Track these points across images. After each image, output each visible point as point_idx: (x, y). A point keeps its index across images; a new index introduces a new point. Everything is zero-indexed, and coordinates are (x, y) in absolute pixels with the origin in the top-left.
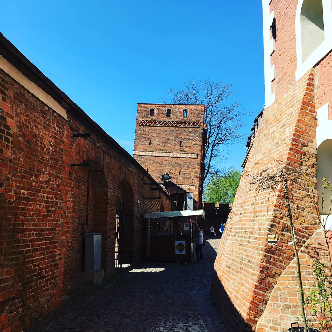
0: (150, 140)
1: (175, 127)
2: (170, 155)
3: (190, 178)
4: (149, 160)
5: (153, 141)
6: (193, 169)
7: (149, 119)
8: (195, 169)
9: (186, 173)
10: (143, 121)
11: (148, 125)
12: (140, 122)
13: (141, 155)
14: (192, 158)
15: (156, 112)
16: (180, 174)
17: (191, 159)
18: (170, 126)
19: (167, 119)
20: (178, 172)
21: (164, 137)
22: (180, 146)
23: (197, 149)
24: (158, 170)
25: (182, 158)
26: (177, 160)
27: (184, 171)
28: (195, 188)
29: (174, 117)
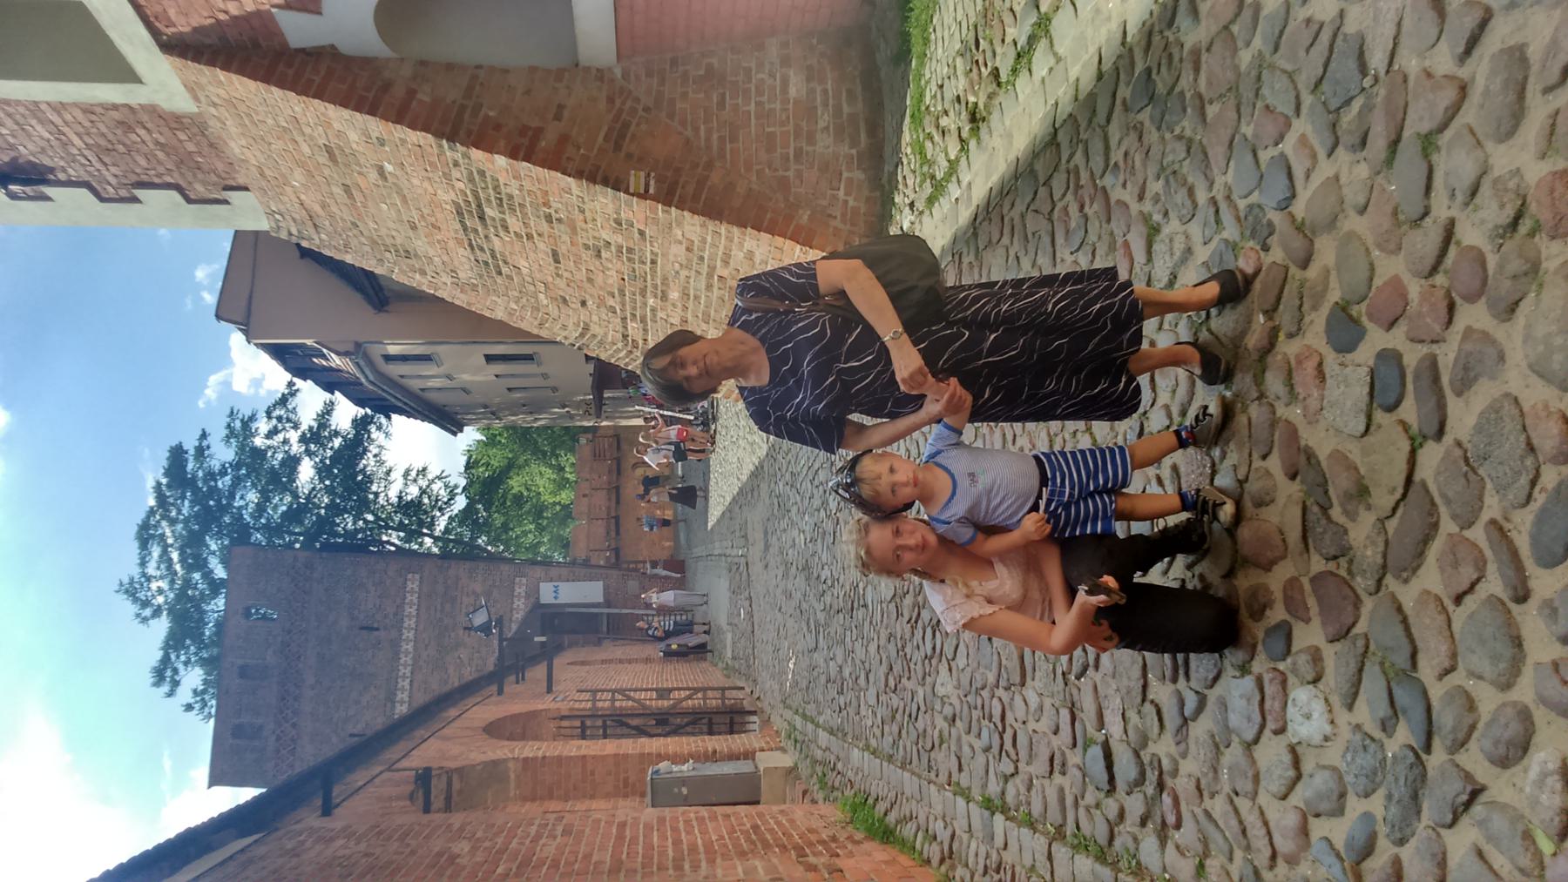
22: (377, 629)
28: (524, 580)
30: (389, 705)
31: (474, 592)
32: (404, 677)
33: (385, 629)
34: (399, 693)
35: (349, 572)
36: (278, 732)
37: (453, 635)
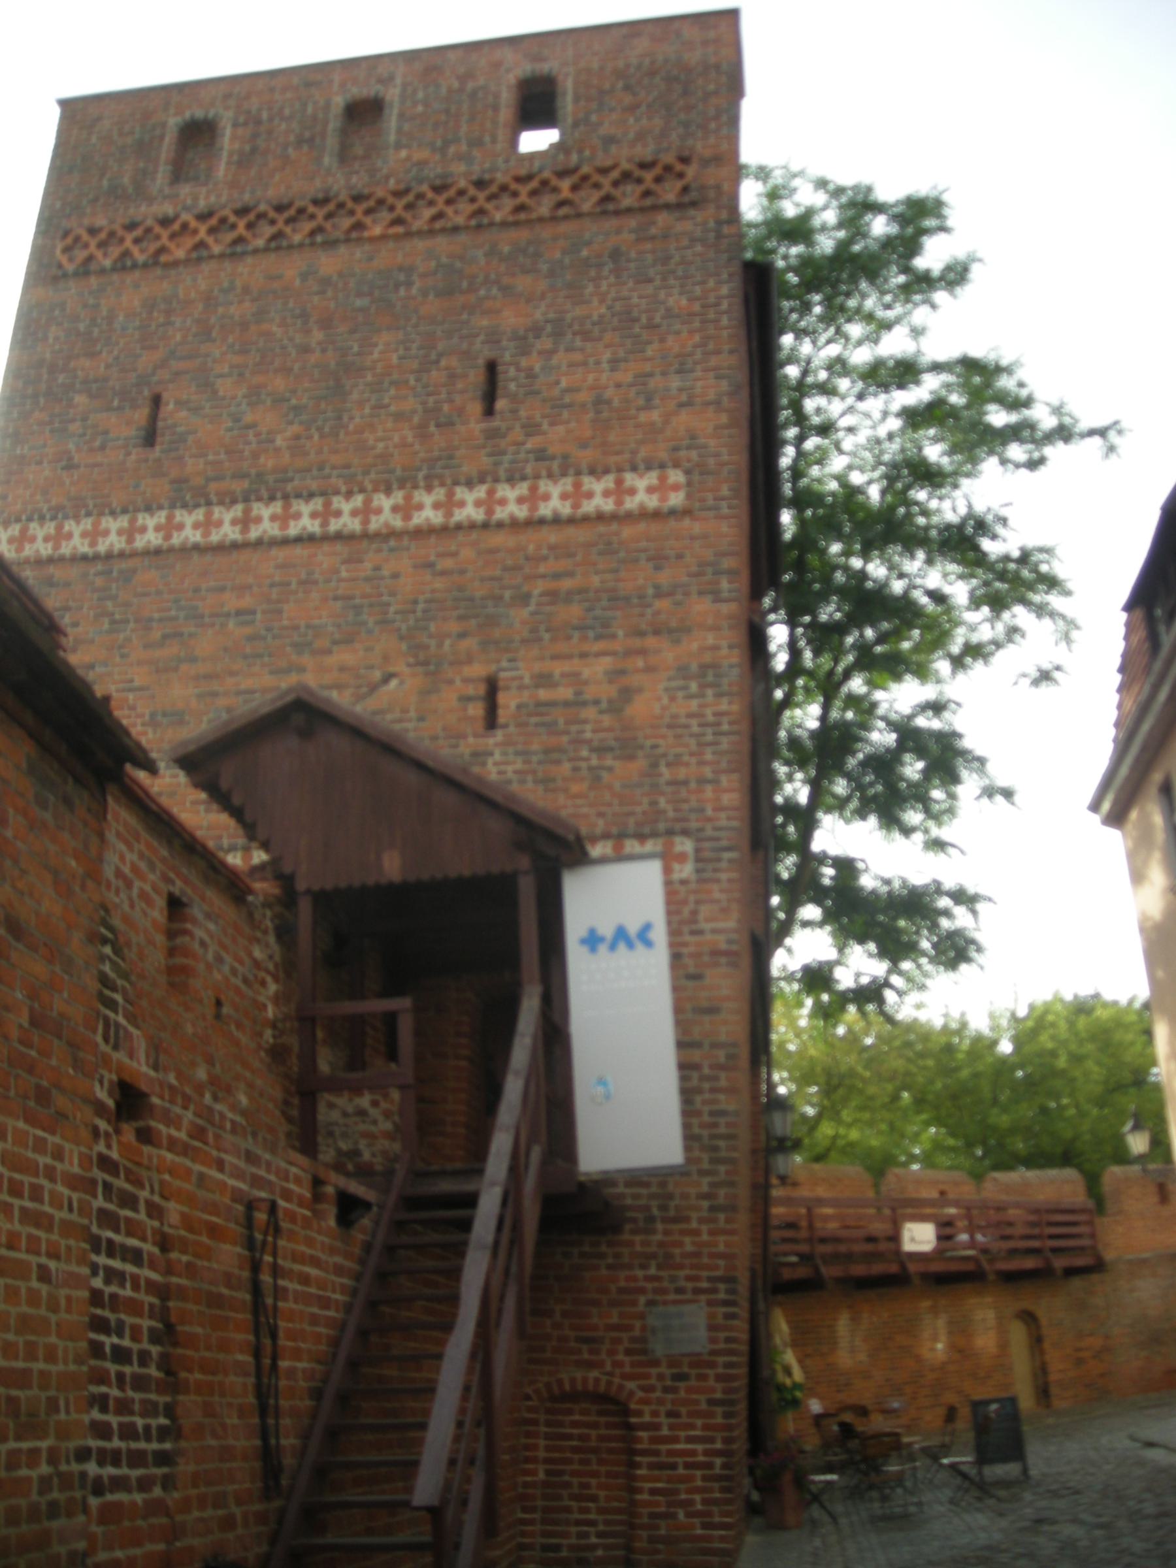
0: (157, 401)
1: (431, 233)
2: (366, 512)
3: (627, 747)
4: (127, 604)
5: (180, 403)
6: (651, 642)
7: (168, 209)
8: (676, 632)
9: (565, 693)
10: (92, 231)
11: (141, 258)
12: (67, 250)
13: (51, 560)
14: (629, 517)
15: (227, 140)
16: (491, 721)
17: (627, 532)
18: (377, 231)
19: (339, 183)
20: (471, 690)
21: (305, 350)
22: (489, 411)
23: (684, 419)
24: (222, 702)
25: (515, 525)
26: (448, 563)
27: (544, 680)
29: (418, 156)
30: (238, 487)
31: (627, 694)
32: (327, 514)
33: (492, 434)
34: (277, 507)
35: (677, 300)
36: (185, 217)
37: (471, 643)
